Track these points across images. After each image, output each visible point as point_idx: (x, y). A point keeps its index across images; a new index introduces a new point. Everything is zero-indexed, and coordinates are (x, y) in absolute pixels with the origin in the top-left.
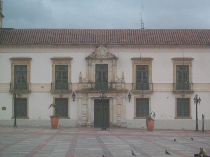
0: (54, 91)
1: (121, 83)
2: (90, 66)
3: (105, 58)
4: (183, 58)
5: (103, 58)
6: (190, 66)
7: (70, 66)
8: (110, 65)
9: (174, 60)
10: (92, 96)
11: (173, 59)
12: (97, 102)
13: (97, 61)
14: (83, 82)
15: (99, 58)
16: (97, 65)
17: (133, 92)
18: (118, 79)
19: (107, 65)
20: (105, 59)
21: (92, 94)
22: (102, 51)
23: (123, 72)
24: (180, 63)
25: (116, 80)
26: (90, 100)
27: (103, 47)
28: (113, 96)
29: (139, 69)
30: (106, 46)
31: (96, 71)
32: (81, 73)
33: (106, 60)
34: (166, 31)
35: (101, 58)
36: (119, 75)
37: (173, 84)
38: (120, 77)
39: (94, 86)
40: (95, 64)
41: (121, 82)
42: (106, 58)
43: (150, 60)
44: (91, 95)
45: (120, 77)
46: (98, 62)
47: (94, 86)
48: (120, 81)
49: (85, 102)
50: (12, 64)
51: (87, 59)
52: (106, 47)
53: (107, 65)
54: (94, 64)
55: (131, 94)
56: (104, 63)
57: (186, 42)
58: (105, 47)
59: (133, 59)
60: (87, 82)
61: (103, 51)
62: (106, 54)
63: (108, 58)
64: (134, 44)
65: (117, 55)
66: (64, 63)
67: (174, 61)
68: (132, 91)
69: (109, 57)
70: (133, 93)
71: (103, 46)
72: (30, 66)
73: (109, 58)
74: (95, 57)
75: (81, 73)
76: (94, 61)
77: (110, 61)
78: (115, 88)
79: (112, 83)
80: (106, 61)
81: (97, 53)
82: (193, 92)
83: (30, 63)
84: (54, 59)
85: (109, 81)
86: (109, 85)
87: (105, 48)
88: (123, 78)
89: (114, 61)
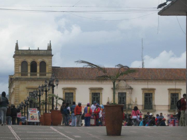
0: (49, 109)
3: (125, 88)
4: (148, 88)
6: (153, 94)
7: (102, 93)
8: (128, 93)
9: (170, 90)
11: (27, 88)
13: (119, 90)
16: (119, 93)
19: (126, 93)
20: (125, 89)
22: (122, 84)
23: (136, 98)
24: (147, 92)
25: (132, 103)
27: (123, 81)
29: (94, 95)
30: (125, 80)
31: (118, 97)
32: (108, 98)
34: (63, 69)
36: (134, 100)
37: (142, 105)
38: (134, 100)
40: (118, 92)
43: (74, 89)
50: (63, 92)
52: (125, 81)
53: (126, 93)
56: (124, 91)
57: (80, 78)
59: (143, 89)
63: (126, 89)
64: (144, 79)
65: (132, 86)
66: (97, 92)
67: (28, 89)
68: (142, 110)
69: (127, 88)
70: (143, 112)
72: (75, 93)
73: (127, 89)
75: (108, 98)
76: (117, 90)
77: (128, 90)
78: (131, 108)
79: (129, 105)
80: (125, 90)
81: (120, 85)
82: (155, 111)
83: (75, 91)
84: (91, 89)
85: (127, 103)
86: (127, 106)
87: (125, 82)
88: (136, 102)
89: (130, 90)
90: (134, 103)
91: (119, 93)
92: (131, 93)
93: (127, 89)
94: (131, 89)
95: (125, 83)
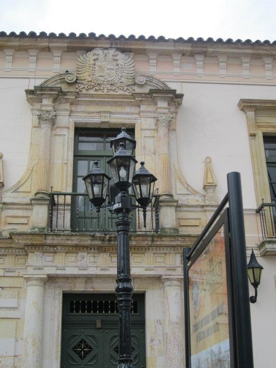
1: (203, 206)
2: (46, 127)
3: (120, 92)
5: (111, 93)
8: (145, 124)
10: (52, 271)
12: (78, 306)
13: (81, 108)
14: (5, 200)
15: (92, 92)
17: (268, 247)
18: (188, 187)
20: (118, 101)
21: (49, 258)
23: (208, 162)
25: (179, 192)
26: (33, 292)
28: (169, 270)
33: (121, 104)
35: (100, 93)
39: (64, 219)
41: (203, 204)
42: (124, 97)
44: (42, 264)
45: (198, 185)
46: (92, 116)
47: (60, 222)
48: (193, 200)
49: (12, 303)
51: (34, 94)
52: (123, 51)
54: (67, 121)
55: (257, 259)
56: (118, 116)
58: (118, 52)
60: (32, 196)
61: (112, 65)
62: (123, 80)
63: (134, 95)
69: (138, 90)
70: (265, 255)
71: (111, 48)
74: (72, 89)
76: (67, 106)
77: (143, 108)
78: (176, 230)
81: (86, 76)
87: (121, 56)
90: (195, 192)
91: (81, 131)
92: (171, 127)
93: (136, 100)
94: (175, 98)
95: (120, 62)
